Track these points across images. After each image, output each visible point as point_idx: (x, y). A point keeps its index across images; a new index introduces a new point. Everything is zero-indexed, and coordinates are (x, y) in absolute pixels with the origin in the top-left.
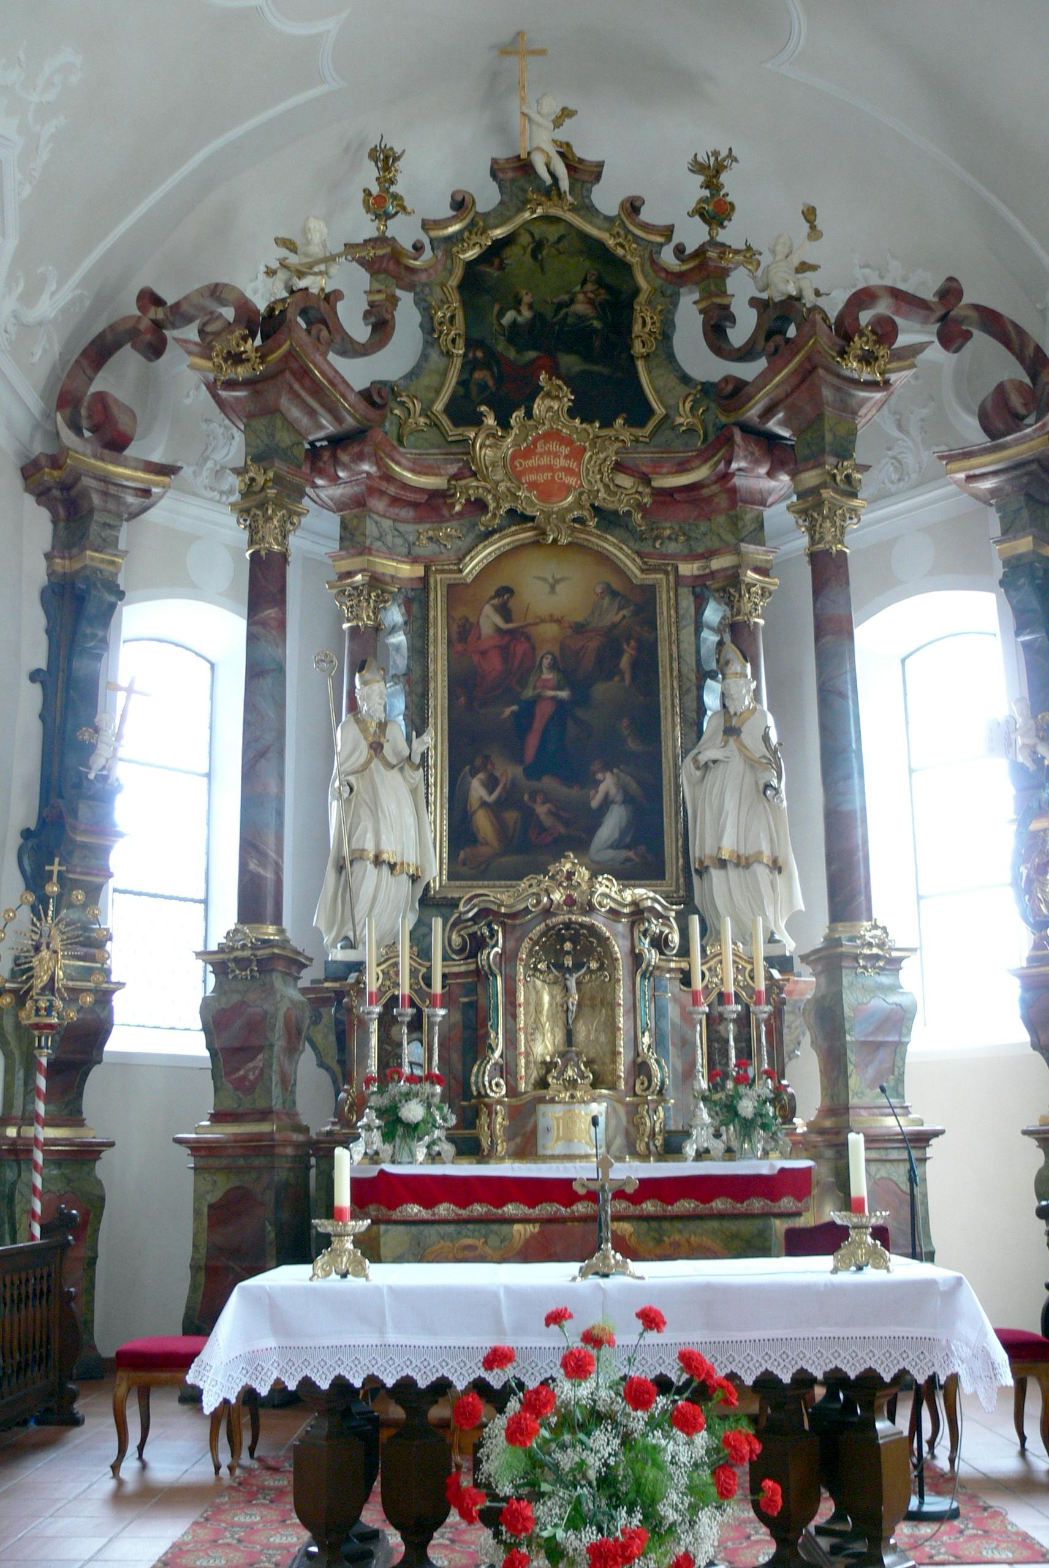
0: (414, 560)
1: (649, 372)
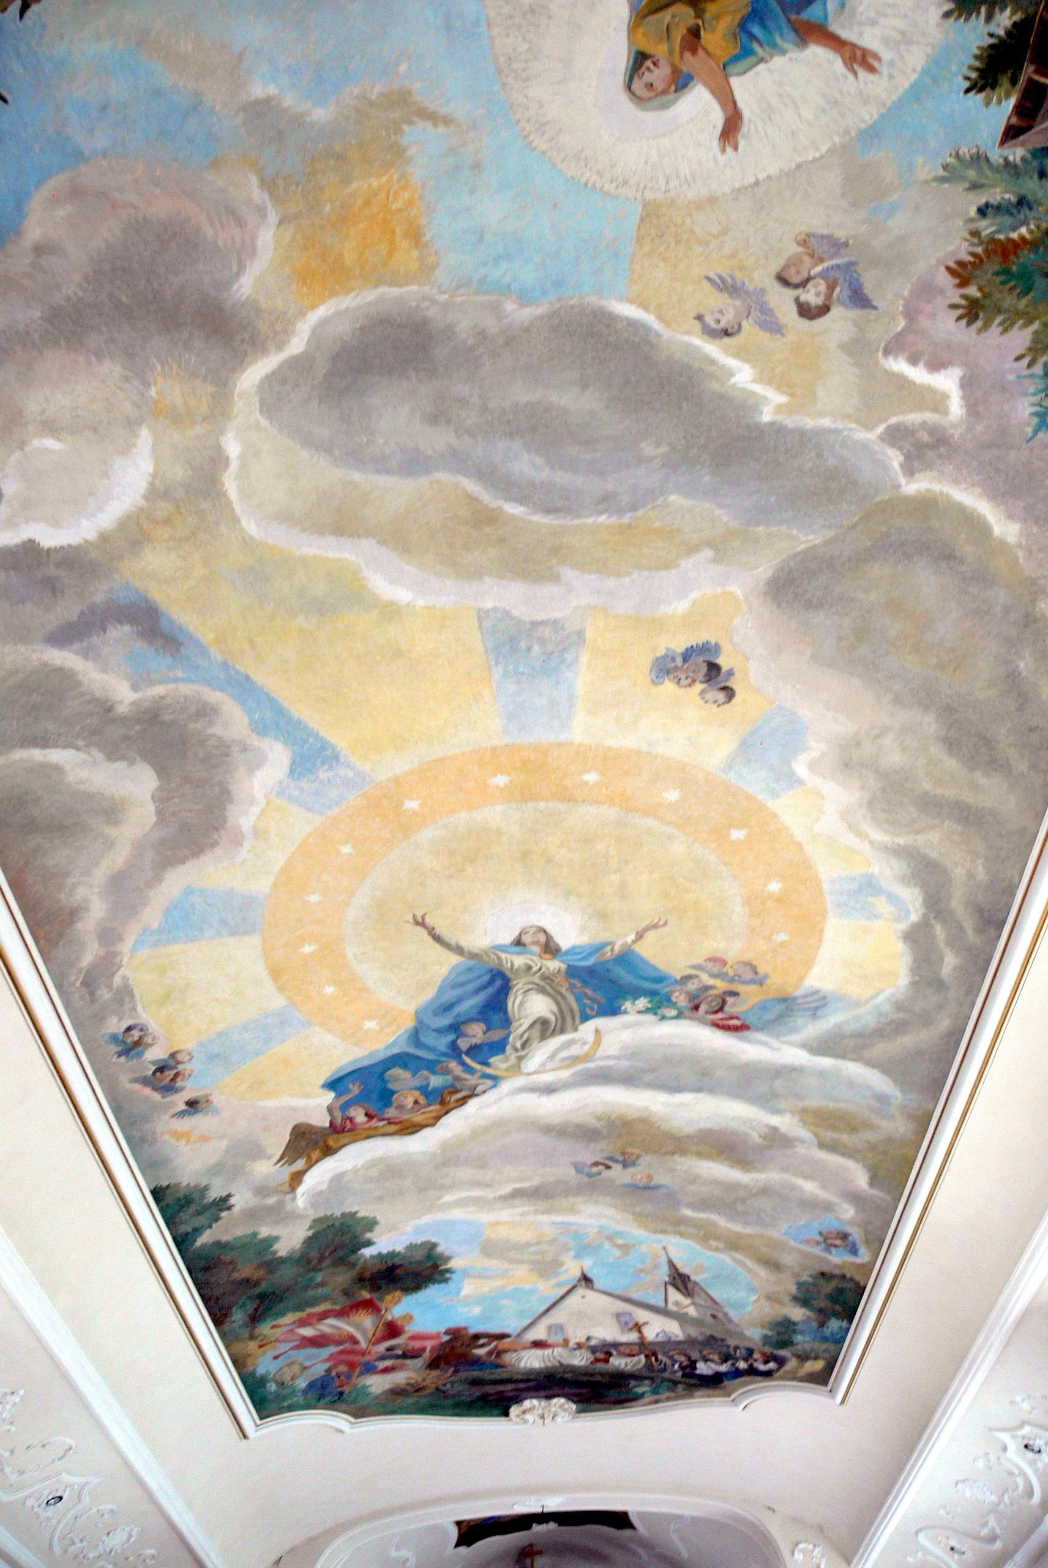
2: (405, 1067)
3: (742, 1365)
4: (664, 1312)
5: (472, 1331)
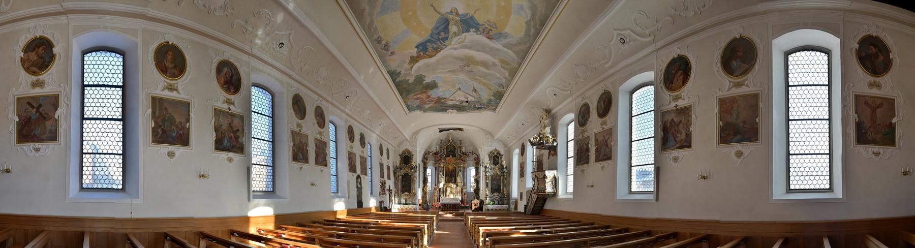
2: (430, 42)
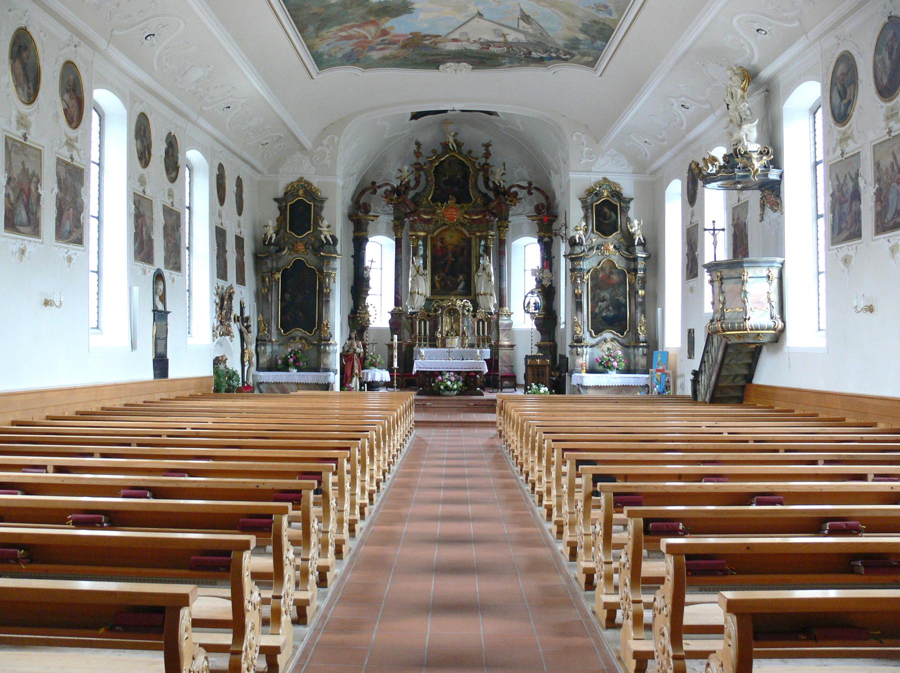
0: (424, 231)
1: (472, 190)
3: (554, 55)
4: (518, 30)
5: (424, 33)
